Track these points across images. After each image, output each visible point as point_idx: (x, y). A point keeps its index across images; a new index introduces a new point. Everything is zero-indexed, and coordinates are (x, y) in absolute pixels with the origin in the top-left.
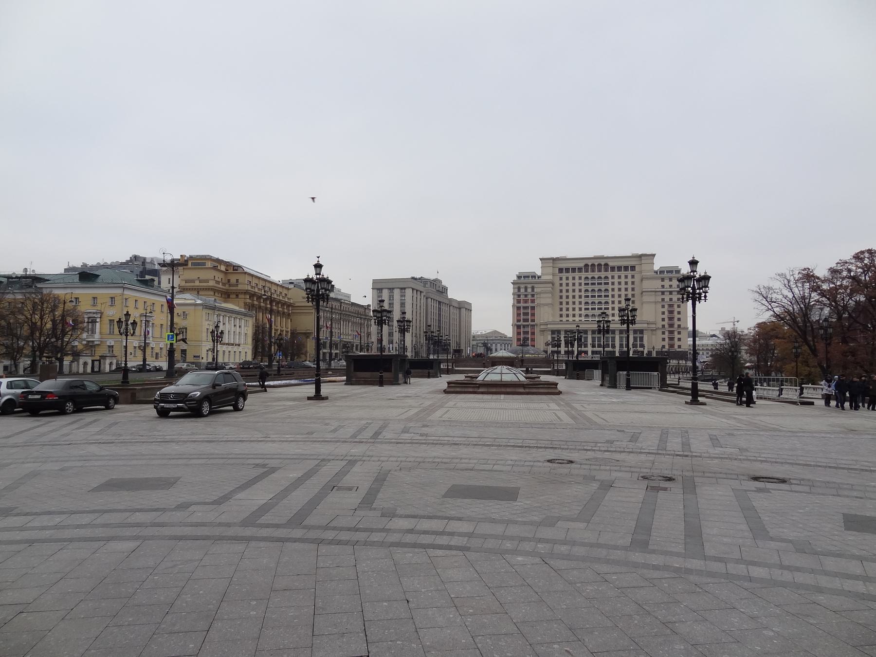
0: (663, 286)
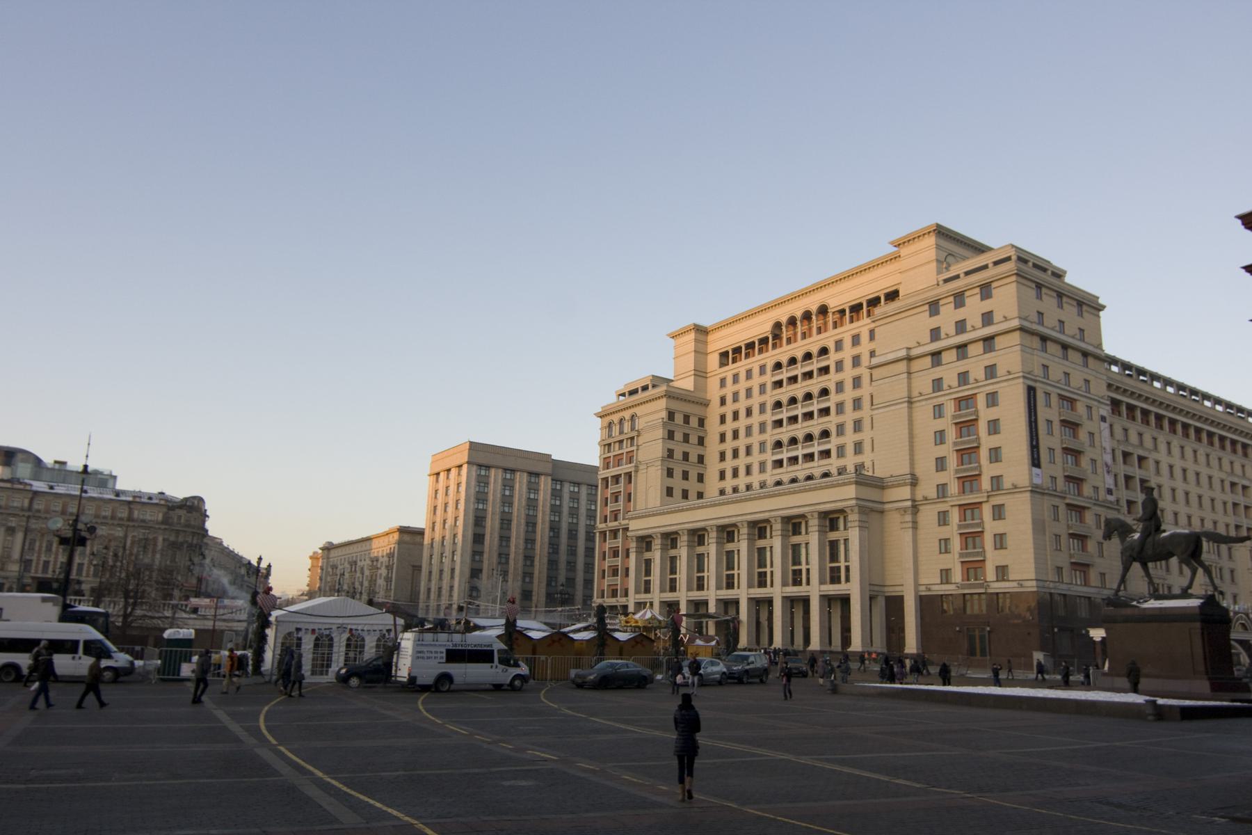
0: (935, 334)
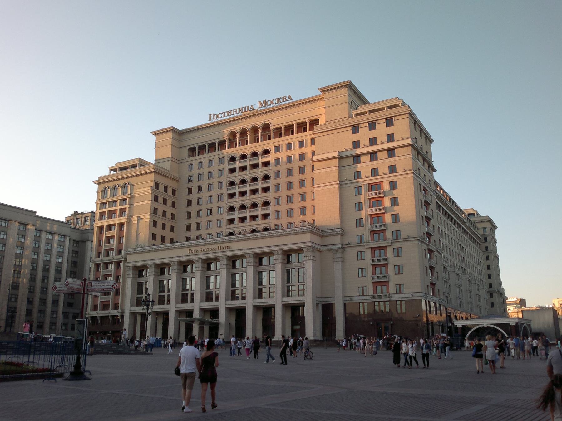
0: (356, 144)
